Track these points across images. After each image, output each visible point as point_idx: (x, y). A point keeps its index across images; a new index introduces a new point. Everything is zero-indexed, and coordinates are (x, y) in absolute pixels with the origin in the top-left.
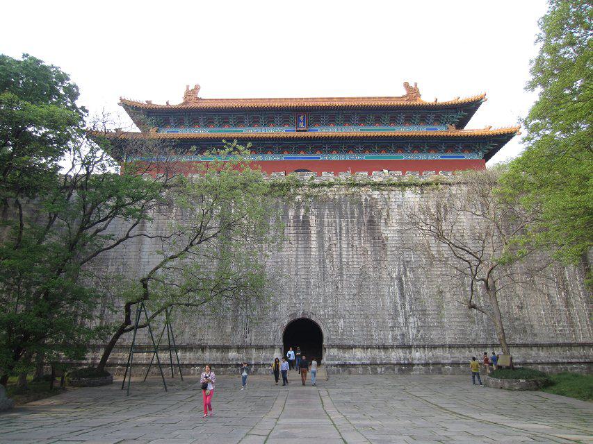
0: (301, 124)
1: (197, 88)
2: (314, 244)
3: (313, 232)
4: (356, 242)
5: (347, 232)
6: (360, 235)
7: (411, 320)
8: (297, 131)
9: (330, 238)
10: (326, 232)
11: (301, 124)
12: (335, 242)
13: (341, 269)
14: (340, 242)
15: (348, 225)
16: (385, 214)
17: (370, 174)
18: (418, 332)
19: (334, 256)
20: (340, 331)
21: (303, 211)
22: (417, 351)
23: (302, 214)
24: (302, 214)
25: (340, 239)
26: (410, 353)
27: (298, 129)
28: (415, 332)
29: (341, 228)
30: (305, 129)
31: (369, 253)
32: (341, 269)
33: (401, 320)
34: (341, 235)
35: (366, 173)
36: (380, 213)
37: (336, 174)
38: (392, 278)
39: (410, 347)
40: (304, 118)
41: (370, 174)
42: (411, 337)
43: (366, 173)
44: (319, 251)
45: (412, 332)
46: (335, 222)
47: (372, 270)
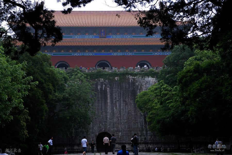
0: (103, 34)
1: (43, 3)
2: (109, 101)
3: (108, 95)
4: (127, 100)
5: (123, 95)
6: (129, 96)
7: (149, 132)
8: (100, 37)
9: (115, 98)
10: (114, 95)
11: (103, 34)
12: (118, 100)
13: (120, 111)
14: (120, 100)
15: (123, 92)
16: (140, 87)
17: (134, 68)
18: (151, 137)
19: (118, 106)
20: (120, 137)
21: (104, 86)
22: (151, 145)
23: (104, 87)
24: (104, 87)
25: (120, 98)
26: (148, 146)
27: (101, 36)
28: (150, 137)
29: (120, 94)
30: (104, 36)
31: (132, 104)
32: (120, 111)
33: (144, 132)
34: (120, 97)
35: (132, 68)
36: (137, 86)
37: (119, 68)
38: (141, 115)
39: (148, 143)
40: (104, 31)
41: (134, 68)
42: (148, 139)
43: (132, 68)
44: (111, 104)
45: (149, 137)
46: (118, 91)
47: (133, 112)
